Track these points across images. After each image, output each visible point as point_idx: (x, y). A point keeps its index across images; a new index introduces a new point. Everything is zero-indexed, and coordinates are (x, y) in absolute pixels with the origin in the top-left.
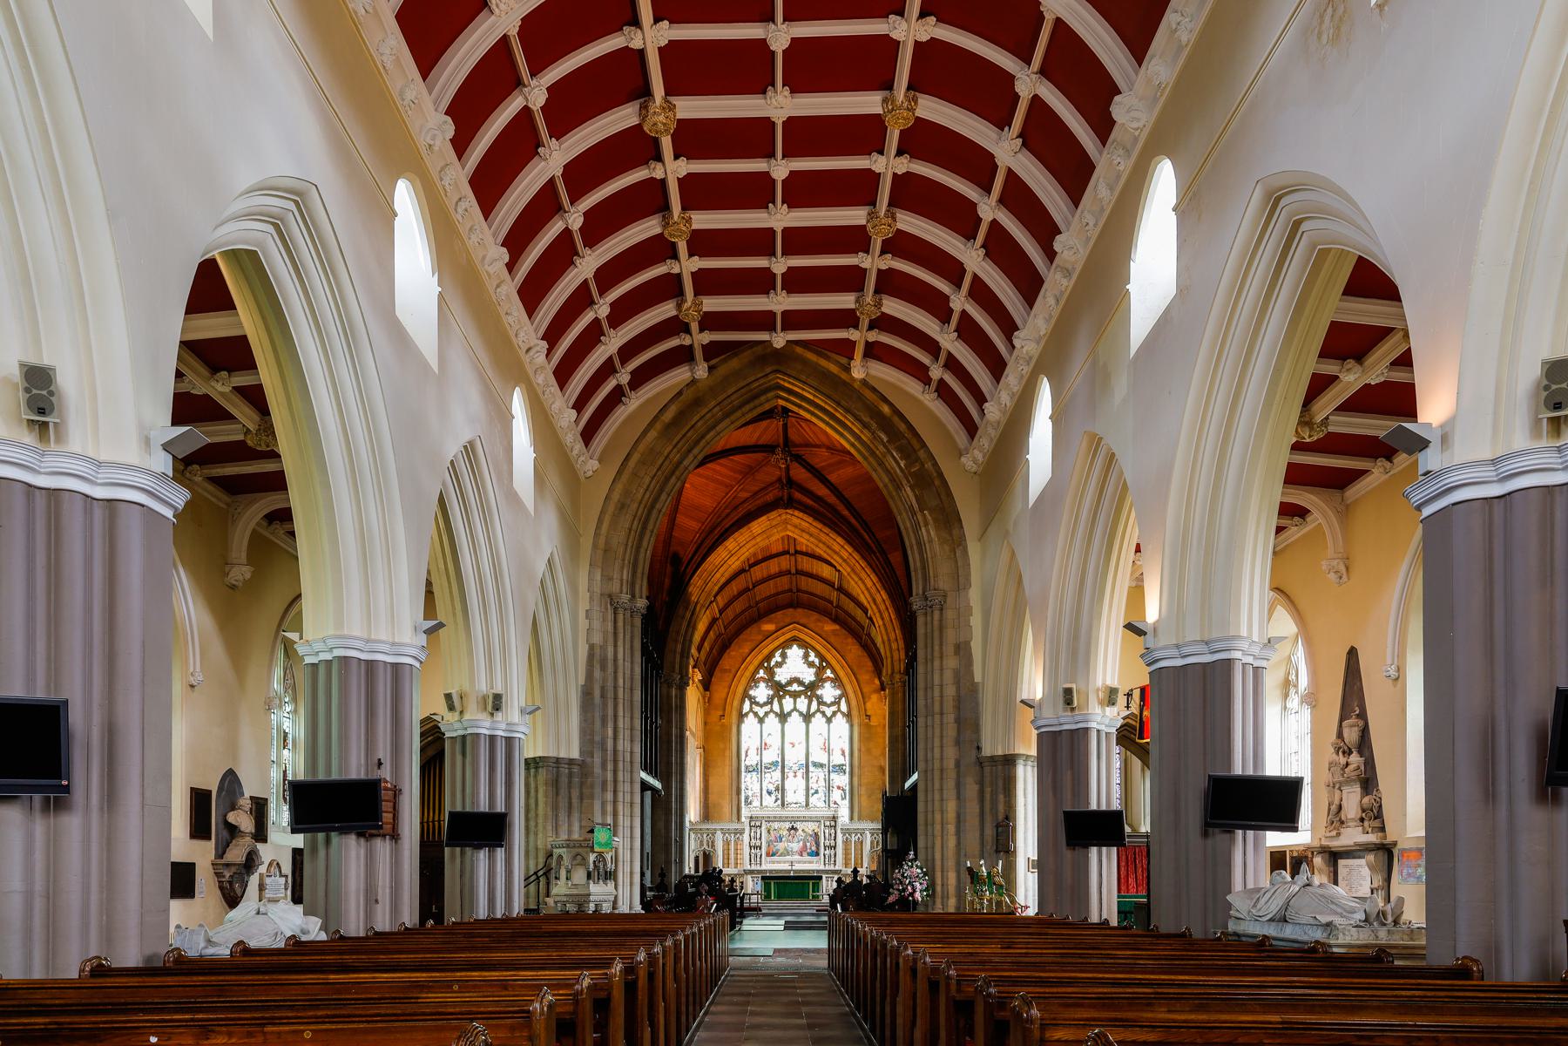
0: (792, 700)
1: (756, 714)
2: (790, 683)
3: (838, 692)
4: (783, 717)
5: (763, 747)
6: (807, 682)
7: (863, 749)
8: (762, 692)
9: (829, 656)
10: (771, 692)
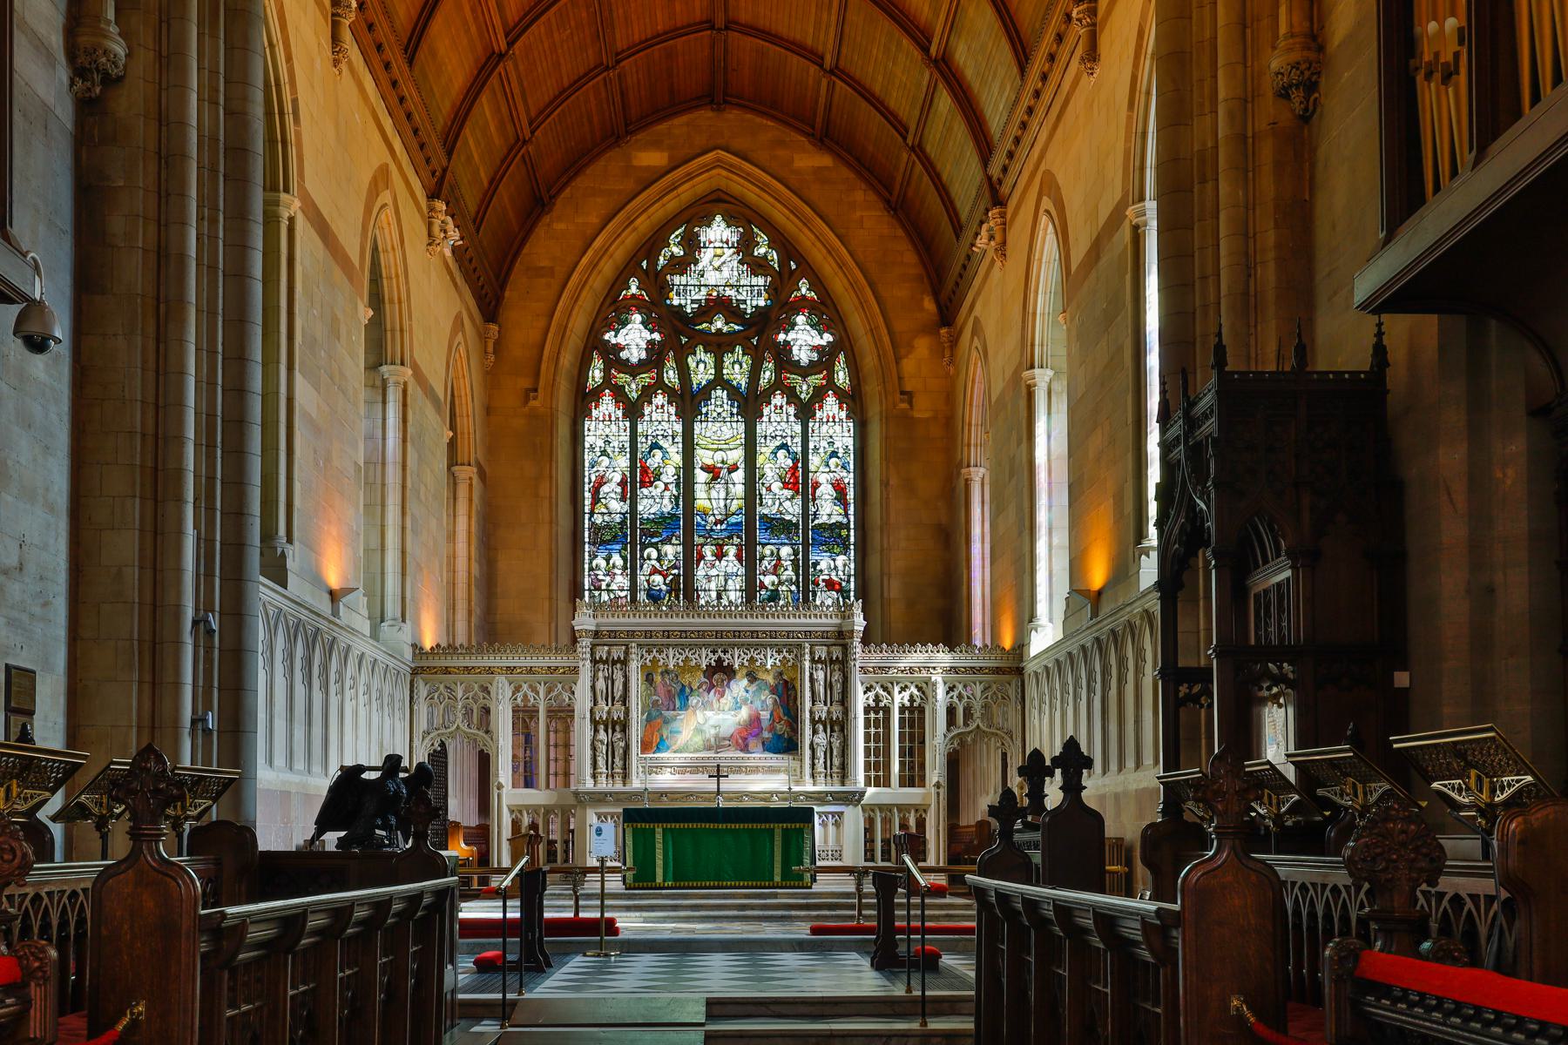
0: (709, 359)
1: (619, 394)
4: (689, 403)
5: (639, 477)
7: (893, 481)
8: (634, 338)
9: (806, 240)
10: (657, 336)
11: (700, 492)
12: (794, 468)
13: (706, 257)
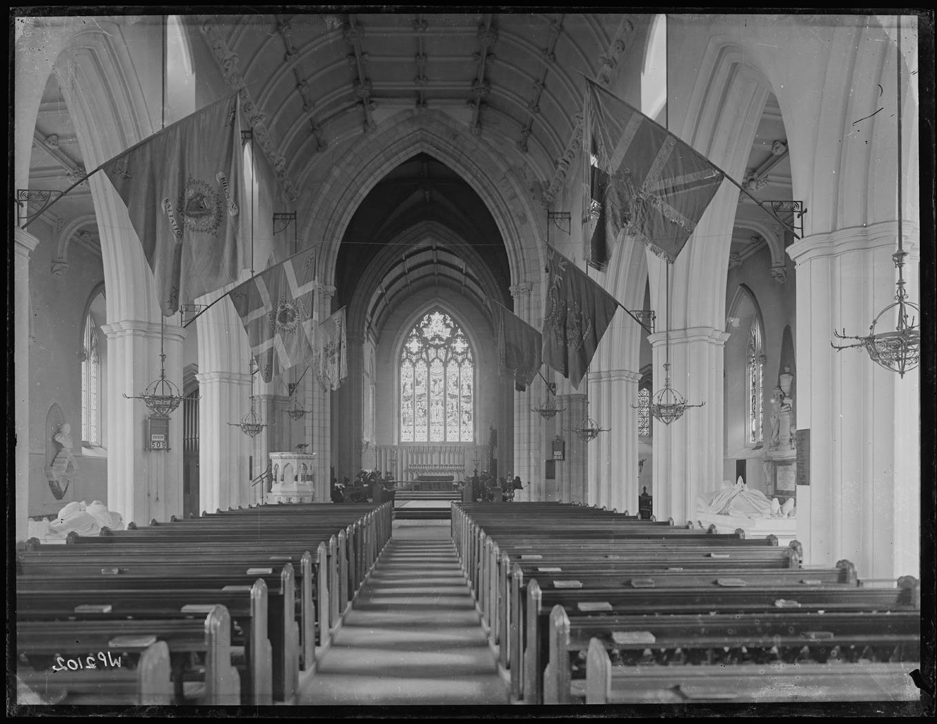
1: (411, 361)
2: (433, 339)
3: (466, 345)
6: (445, 338)
8: (414, 345)
10: (421, 345)
11: (432, 387)
12: (457, 381)
13: (433, 323)
